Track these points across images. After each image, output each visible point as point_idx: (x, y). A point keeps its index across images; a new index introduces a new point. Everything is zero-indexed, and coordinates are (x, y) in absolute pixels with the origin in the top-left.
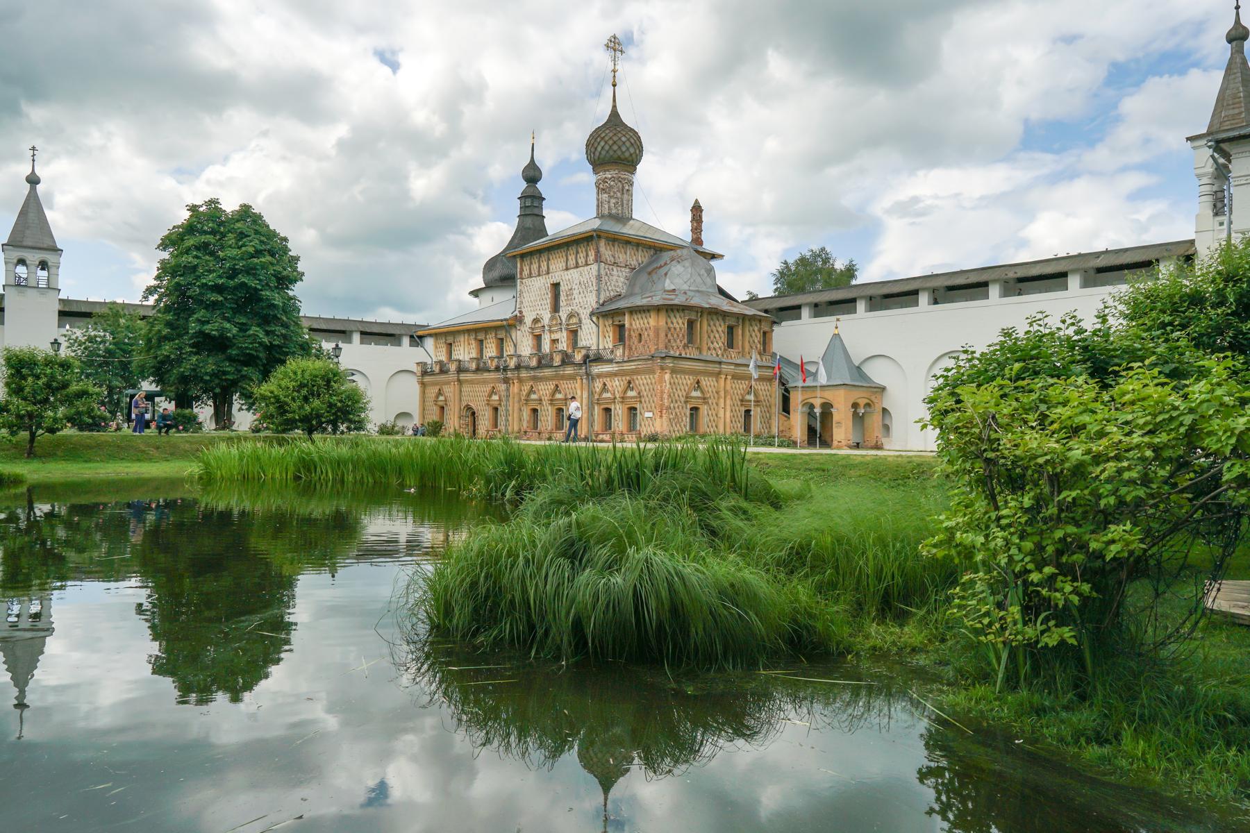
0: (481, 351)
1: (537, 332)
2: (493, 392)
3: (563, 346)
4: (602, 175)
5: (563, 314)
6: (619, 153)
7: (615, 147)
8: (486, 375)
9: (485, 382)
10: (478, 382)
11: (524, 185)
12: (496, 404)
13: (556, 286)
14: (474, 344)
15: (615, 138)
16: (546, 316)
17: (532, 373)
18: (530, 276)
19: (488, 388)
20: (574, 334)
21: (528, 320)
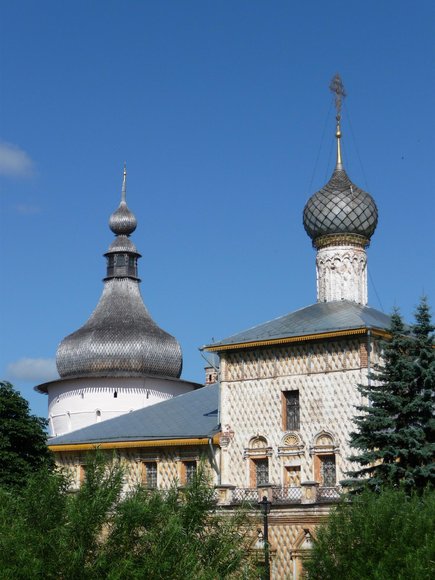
5: (307, 433)
7: (353, 217)
13: (292, 395)
16: (276, 437)
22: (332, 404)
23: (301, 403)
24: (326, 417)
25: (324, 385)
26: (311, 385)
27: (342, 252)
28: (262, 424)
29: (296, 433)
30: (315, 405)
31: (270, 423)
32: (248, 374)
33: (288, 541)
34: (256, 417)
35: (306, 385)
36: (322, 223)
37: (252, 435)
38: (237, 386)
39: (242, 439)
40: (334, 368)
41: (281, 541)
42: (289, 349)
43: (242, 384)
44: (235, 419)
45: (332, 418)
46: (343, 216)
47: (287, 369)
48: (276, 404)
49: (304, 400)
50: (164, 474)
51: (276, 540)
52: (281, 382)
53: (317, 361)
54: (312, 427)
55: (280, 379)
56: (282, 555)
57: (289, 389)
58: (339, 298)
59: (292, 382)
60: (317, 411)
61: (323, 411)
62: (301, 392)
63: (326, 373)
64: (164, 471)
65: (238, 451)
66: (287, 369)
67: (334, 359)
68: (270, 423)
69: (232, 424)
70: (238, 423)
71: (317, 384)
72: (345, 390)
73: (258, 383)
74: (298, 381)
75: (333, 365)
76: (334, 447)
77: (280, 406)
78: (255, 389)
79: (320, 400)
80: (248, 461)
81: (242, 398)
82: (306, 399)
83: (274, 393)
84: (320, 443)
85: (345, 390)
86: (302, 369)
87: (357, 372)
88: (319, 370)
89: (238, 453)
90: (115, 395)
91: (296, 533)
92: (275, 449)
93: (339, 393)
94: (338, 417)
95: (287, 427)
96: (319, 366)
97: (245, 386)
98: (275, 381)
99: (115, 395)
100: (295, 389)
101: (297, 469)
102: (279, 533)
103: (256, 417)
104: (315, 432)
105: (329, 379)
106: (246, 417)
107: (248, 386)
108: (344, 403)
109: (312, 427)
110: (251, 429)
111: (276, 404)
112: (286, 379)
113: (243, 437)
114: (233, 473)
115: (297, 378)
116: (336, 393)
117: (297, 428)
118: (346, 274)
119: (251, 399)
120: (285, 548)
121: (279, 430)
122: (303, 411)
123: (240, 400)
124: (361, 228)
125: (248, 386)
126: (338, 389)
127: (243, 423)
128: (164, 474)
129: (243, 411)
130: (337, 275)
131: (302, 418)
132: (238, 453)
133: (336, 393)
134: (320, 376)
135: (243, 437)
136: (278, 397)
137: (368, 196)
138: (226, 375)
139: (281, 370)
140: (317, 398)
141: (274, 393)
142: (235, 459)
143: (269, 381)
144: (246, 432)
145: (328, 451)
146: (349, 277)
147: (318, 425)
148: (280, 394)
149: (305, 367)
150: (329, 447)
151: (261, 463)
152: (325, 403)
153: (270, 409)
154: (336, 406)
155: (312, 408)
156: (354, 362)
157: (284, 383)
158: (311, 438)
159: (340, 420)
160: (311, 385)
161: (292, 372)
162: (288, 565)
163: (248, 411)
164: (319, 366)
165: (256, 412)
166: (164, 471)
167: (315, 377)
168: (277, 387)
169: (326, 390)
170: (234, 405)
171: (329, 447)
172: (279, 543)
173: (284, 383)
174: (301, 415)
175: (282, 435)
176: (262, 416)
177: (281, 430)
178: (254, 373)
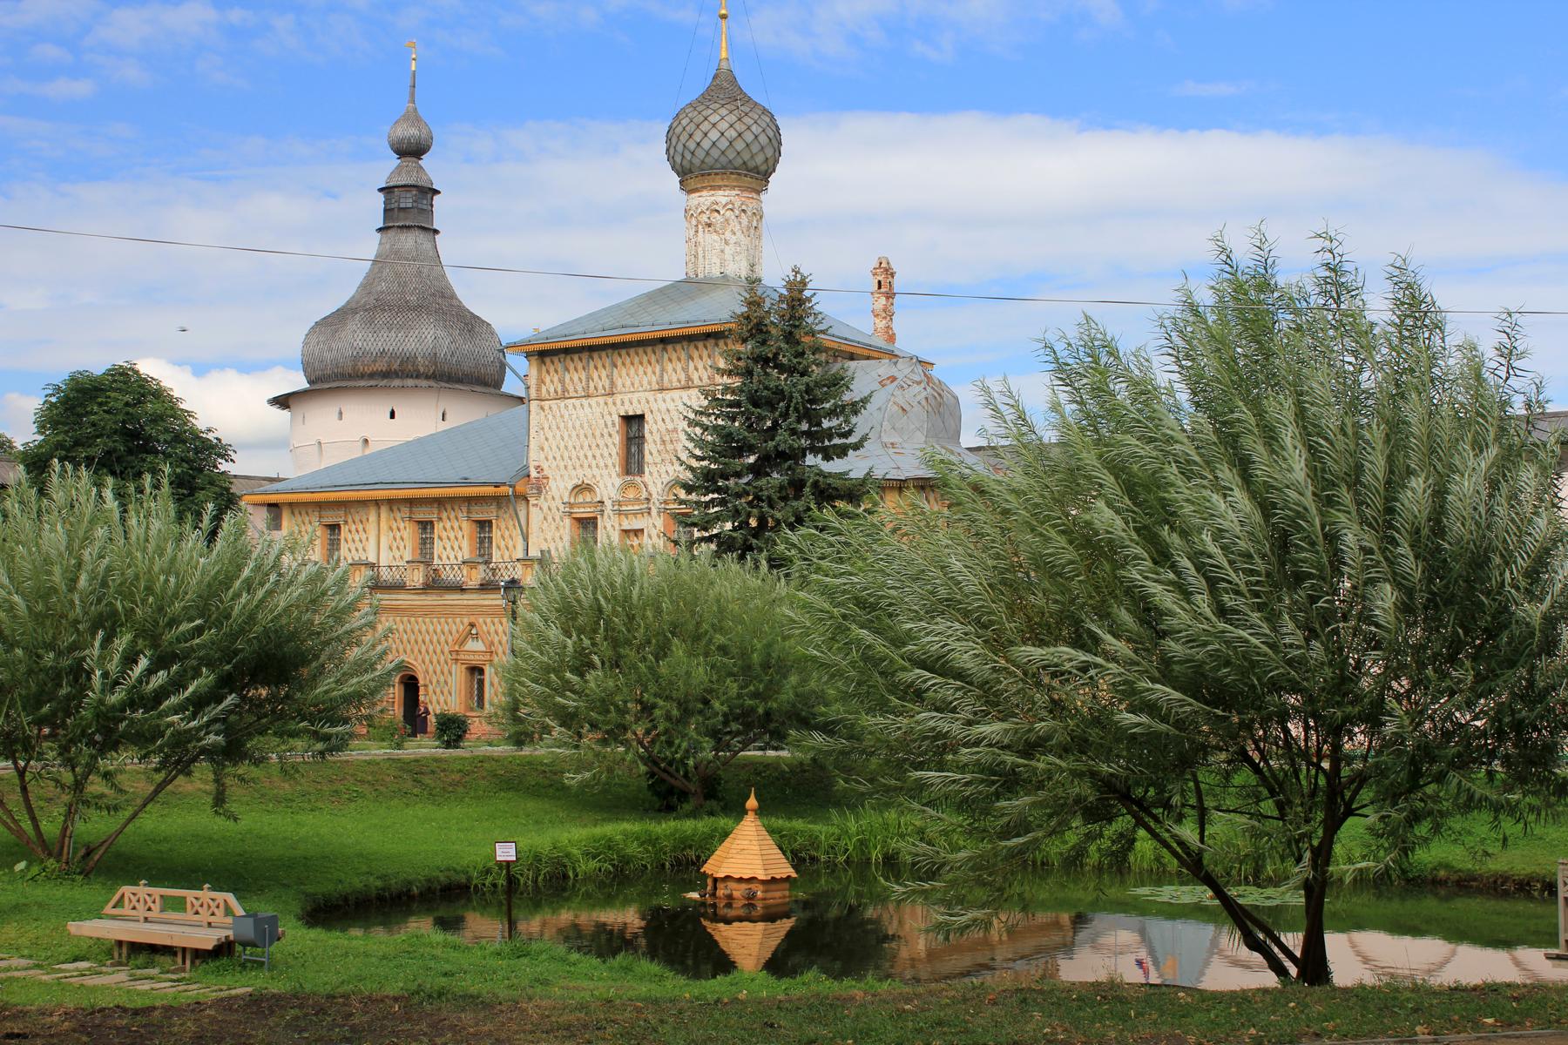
0: (426, 544)
2: (472, 632)
4: (695, 199)
6: (746, 156)
7: (740, 145)
8: (452, 598)
9: (450, 613)
10: (428, 612)
11: (394, 161)
12: (476, 660)
13: (633, 422)
14: (409, 532)
15: (740, 127)
16: (609, 484)
18: (563, 396)
19: (460, 625)
21: (560, 486)
23: (647, 435)
26: (663, 407)
27: (724, 200)
29: (638, 479)
30: (667, 438)
31: (602, 464)
32: (571, 388)
34: (581, 455)
35: (655, 409)
37: (576, 482)
38: (555, 408)
39: (560, 486)
40: (697, 382)
42: (632, 351)
46: (723, 144)
49: (651, 429)
54: (663, 470)
55: (618, 398)
58: (716, 272)
59: (635, 402)
66: (628, 383)
68: (602, 464)
69: (545, 465)
77: (617, 439)
78: (581, 412)
80: (567, 521)
82: (654, 429)
83: (607, 418)
88: (676, 384)
90: (392, 415)
92: (608, 503)
95: (627, 470)
96: (674, 379)
98: (610, 400)
99: (392, 415)
100: (639, 412)
101: (638, 532)
103: (581, 455)
104: (666, 479)
106: (566, 455)
109: (663, 470)
112: (626, 398)
113: (562, 486)
117: (641, 472)
118: (728, 235)
122: (649, 447)
124: (751, 164)
130: (715, 237)
131: (648, 458)
134: (676, 394)
135: (562, 486)
137: (765, 111)
138: (539, 390)
139: (619, 382)
140: (670, 427)
141: (607, 418)
143: (601, 400)
146: (733, 239)
148: (617, 420)
149: (654, 379)
151: (587, 524)
153: (601, 443)
155: (664, 442)
158: (660, 486)
160: (663, 407)
163: (570, 445)
164: (674, 379)
166: (444, 535)
167: (668, 395)
168: (613, 410)
170: (550, 435)
174: (646, 452)
175: (618, 482)
176: (589, 454)
178: (580, 389)
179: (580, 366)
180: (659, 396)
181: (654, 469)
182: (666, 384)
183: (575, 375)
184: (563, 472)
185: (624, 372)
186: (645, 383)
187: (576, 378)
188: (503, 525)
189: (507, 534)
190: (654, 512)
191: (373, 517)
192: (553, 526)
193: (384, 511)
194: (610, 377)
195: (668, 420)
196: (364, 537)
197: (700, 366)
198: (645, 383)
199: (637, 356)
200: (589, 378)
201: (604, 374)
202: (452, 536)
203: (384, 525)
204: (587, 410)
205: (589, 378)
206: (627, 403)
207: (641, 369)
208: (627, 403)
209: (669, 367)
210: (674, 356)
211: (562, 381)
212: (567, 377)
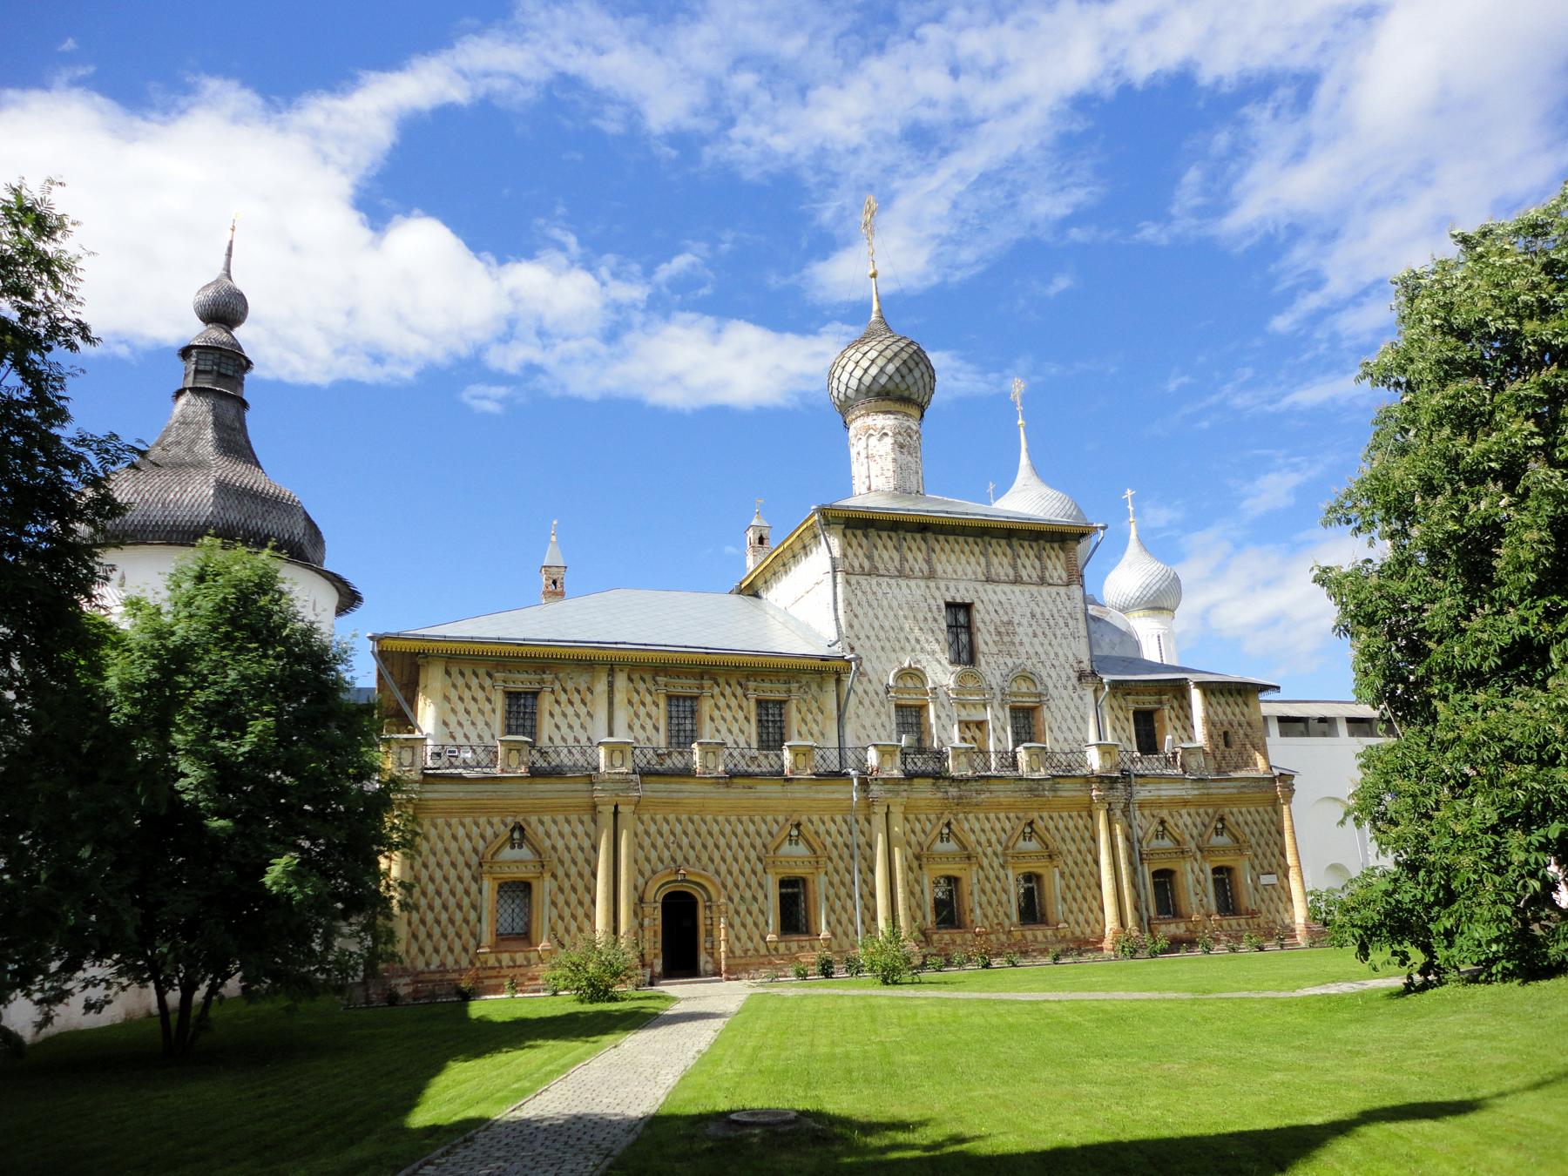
1: (910, 699)
3: (999, 738)
16: (941, 673)
17: (953, 791)
18: (873, 572)
20: (1025, 721)
22: (1030, 631)
23: (980, 624)
24: (1022, 650)
25: (1014, 602)
28: (913, 650)
30: (1002, 630)
33: (994, 839)
34: (902, 636)
35: (985, 599)
36: (903, 377)
38: (864, 583)
40: (1025, 578)
41: (983, 839)
43: (874, 581)
44: (862, 636)
45: (1031, 652)
47: (949, 570)
48: (935, 620)
50: (719, 722)
51: (973, 838)
52: (943, 587)
53: (1001, 564)
54: (1001, 661)
56: (985, 862)
57: (959, 600)
59: (961, 588)
60: (1006, 639)
61: (1017, 640)
62: (978, 605)
63: (1015, 582)
64: (716, 714)
65: (870, 689)
66: (949, 570)
67: (1029, 565)
70: (868, 644)
71: (1003, 598)
72: (1048, 615)
73: (903, 582)
74: (972, 591)
75: (1024, 574)
76: (1040, 695)
77: (944, 626)
79: (1010, 623)
81: (875, 604)
82: (987, 618)
84: (1014, 689)
85: (1048, 615)
86: (974, 573)
87: (1062, 590)
89: (872, 694)
91: (1008, 826)
93: (1038, 616)
94: (1040, 650)
97: (879, 584)
98: (932, 585)
100: (968, 601)
101: (980, 725)
102: (977, 827)
105: (1022, 593)
106: (882, 635)
107: (884, 585)
108: (1047, 632)
110: (893, 656)
111: (935, 620)
112: (952, 585)
114: (864, 727)
115: (971, 585)
116: (1033, 616)
117: (972, 660)
119: (891, 607)
120: (989, 851)
121: (945, 662)
123: (870, 606)
125: (884, 585)
126: (1038, 611)
127: (878, 645)
128: (719, 722)
129: (876, 624)
132: (872, 694)
133: (1033, 616)
134: (1007, 588)
136: (939, 610)
140: (1005, 619)
141: (932, 601)
142: (867, 702)
143: (922, 583)
144: (884, 659)
145: (1029, 701)
147: (1010, 662)
149: (979, 570)
150: (1030, 695)
152: (1020, 630)
154: (1035, 635)
155: (999, 633)
156: (1055, 575)
157: (948, 589)
159: (1043, 657)
160: (995, 599)
161: (960, 573)
162: (998, 878)
163: (887, 625)
165: (902, 629)
166: (716, 714)
167: (999, 588)
168: (937, 594)
169: (1019, 611)
170: (859, 611)
171: (1030, 695)
172: (979, 843)
173: (948, 589)
177: (951, 663)
179: (890, 544)
180: (989, 587)
181: (991, 660)
182: (994, 576)
183: (886, 553)
184: (881, 654)
185: (943, 557)
186: (969, 570)
187: (886, 555)
188: (804, 709)
189: (809, 717)
190: (996, 704)
191: (601, 687)
192: (872, 712)
193: (621, 681)
194: (928, 562)
195: (1001, 612)
196: (583, 710)
197: (1028, 564)
198: (969, 570)
199: (958, 544)
200: (903, 559)
201: (920, 557)
202: (728, 715)
203: (620, 697)
204: (906, 591)
205: (903, 559)
206: (953, 590)
207: (963, 559)
208: (953, 590)
209: (995, 561)
210: (999, 551)
211: (870, 558)
212: (876, 554)
